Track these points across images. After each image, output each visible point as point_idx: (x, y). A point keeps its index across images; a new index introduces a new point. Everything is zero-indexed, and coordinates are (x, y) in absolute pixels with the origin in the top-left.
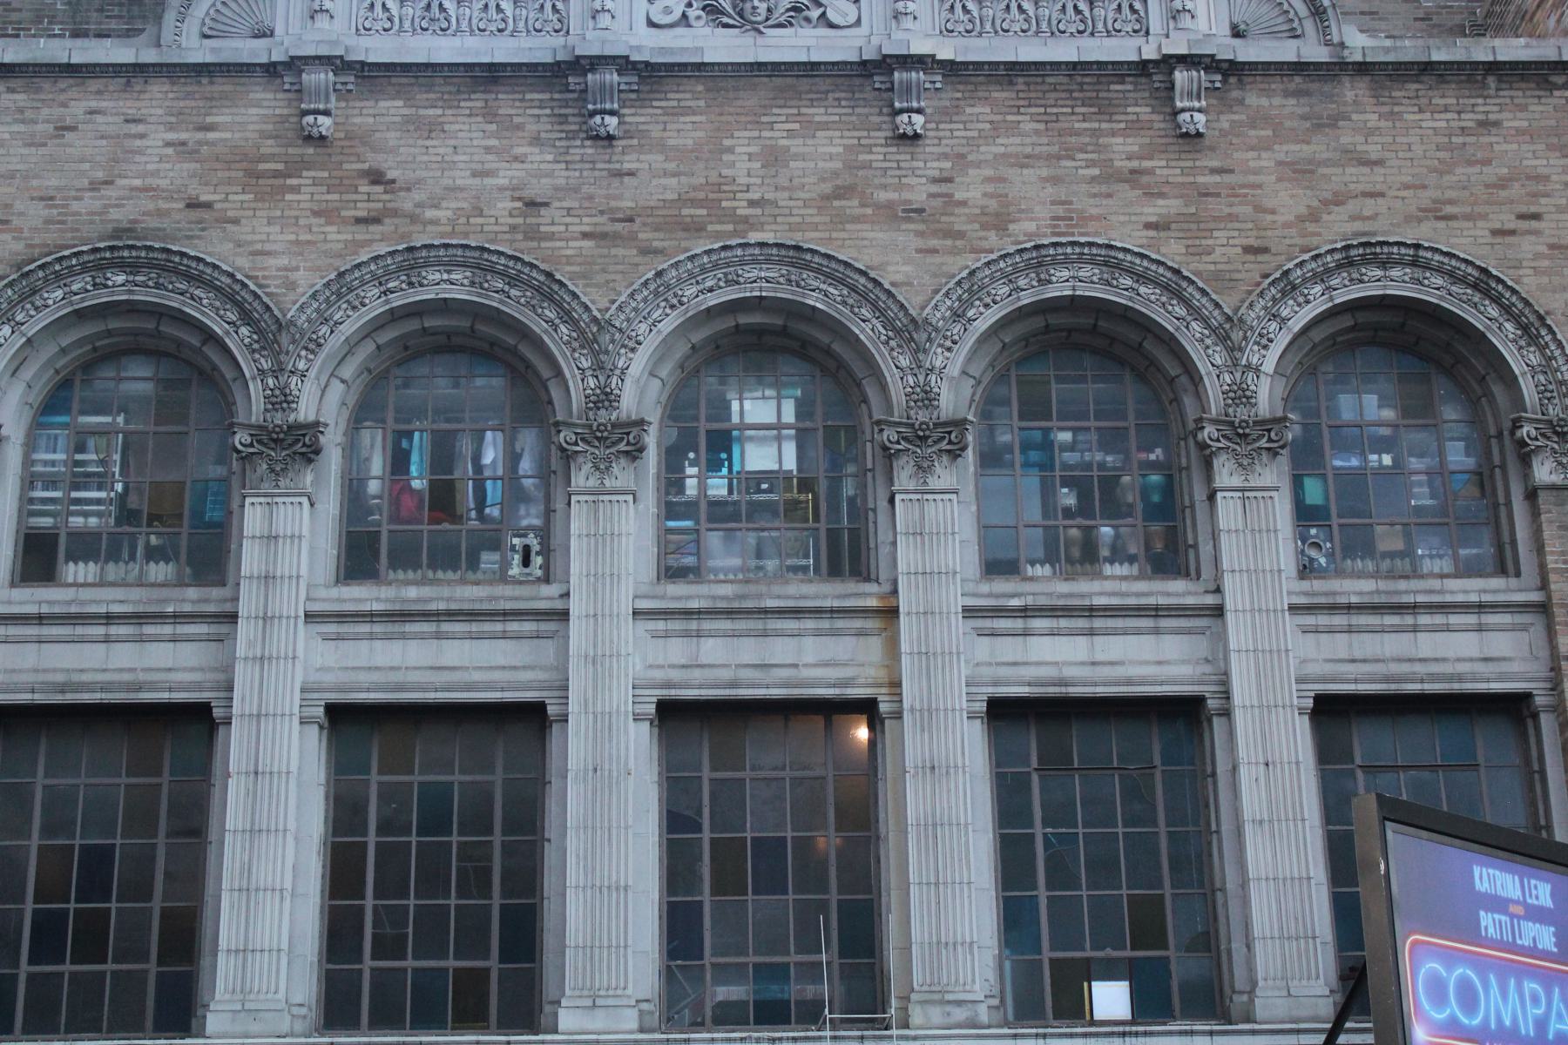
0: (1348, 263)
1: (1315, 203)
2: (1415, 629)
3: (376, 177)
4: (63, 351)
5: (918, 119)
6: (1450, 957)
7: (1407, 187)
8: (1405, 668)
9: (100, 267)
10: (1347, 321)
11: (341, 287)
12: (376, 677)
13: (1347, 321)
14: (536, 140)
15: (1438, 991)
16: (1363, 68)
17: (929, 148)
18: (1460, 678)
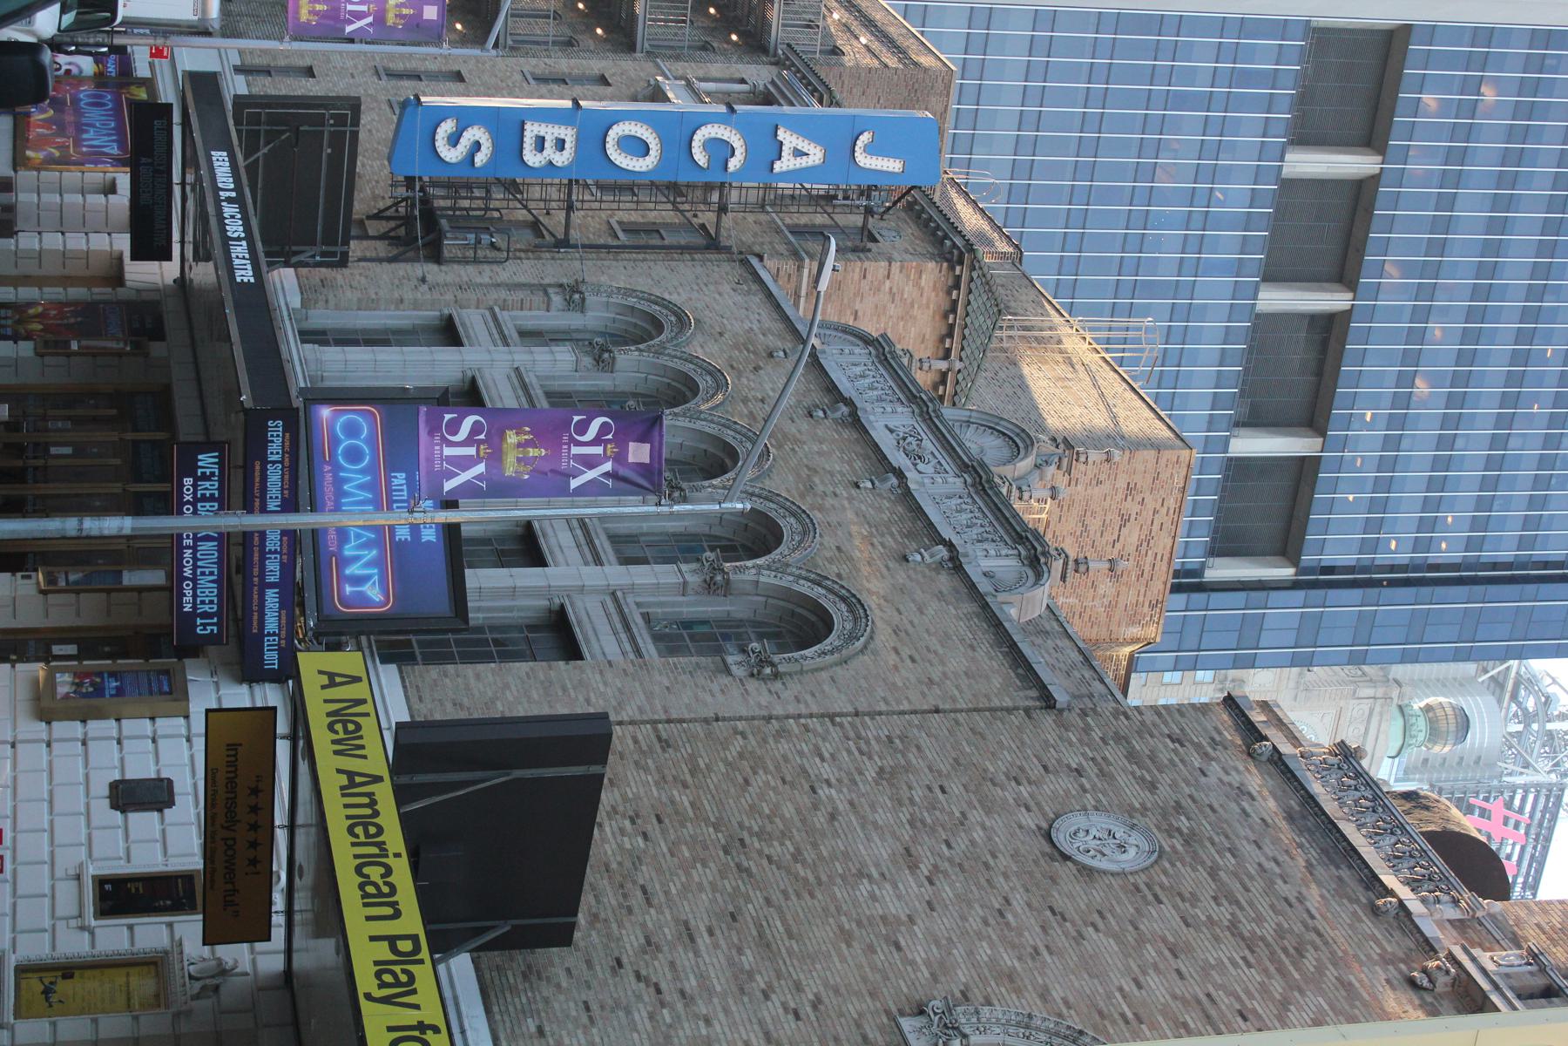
0: (843, 599)
1: (882, 592)
2: (615, 633)
3: (757, 369)
4: (636, 325)
5: (869, 485)
6: (372, 441)
7: (911, 622)
8: (588, 627)
9: (675, 314)
10: (813, 618)
11: (691, 359)
12: (491, 384)
13: (813, 618)
14: (799, 402)
15: (352, 430)
16: (985, 606)
17: (854, 492)
18: (587, 641)
